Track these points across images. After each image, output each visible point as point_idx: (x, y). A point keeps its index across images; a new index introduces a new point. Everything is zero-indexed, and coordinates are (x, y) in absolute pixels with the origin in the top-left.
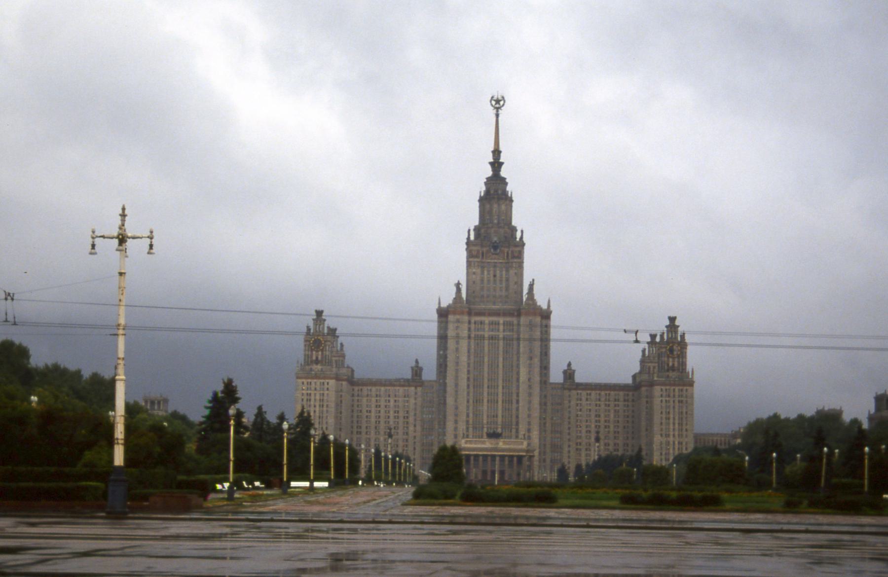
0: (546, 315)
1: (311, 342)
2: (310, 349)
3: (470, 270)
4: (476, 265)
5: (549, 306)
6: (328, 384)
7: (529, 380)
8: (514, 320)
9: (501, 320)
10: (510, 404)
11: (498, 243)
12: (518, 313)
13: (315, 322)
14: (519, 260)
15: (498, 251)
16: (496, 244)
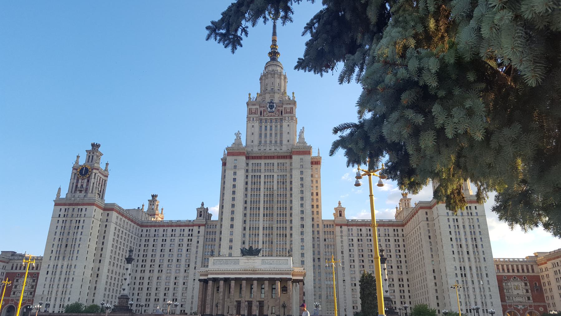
0: (316, 162)
1: (79, 170)
2: (76, 178)
3: (249, 124)
4: (255, 120)
5: (319, 153)
6: (86, 209)
7: (302, 212)
8: (287, 161)
9: (275, 161)
10: (284, 238)
11: (273, 103)
12: (291, 157)
13: (88, 153)
14: (292, 115)
15: (274, 109)
16: (271, 104)
